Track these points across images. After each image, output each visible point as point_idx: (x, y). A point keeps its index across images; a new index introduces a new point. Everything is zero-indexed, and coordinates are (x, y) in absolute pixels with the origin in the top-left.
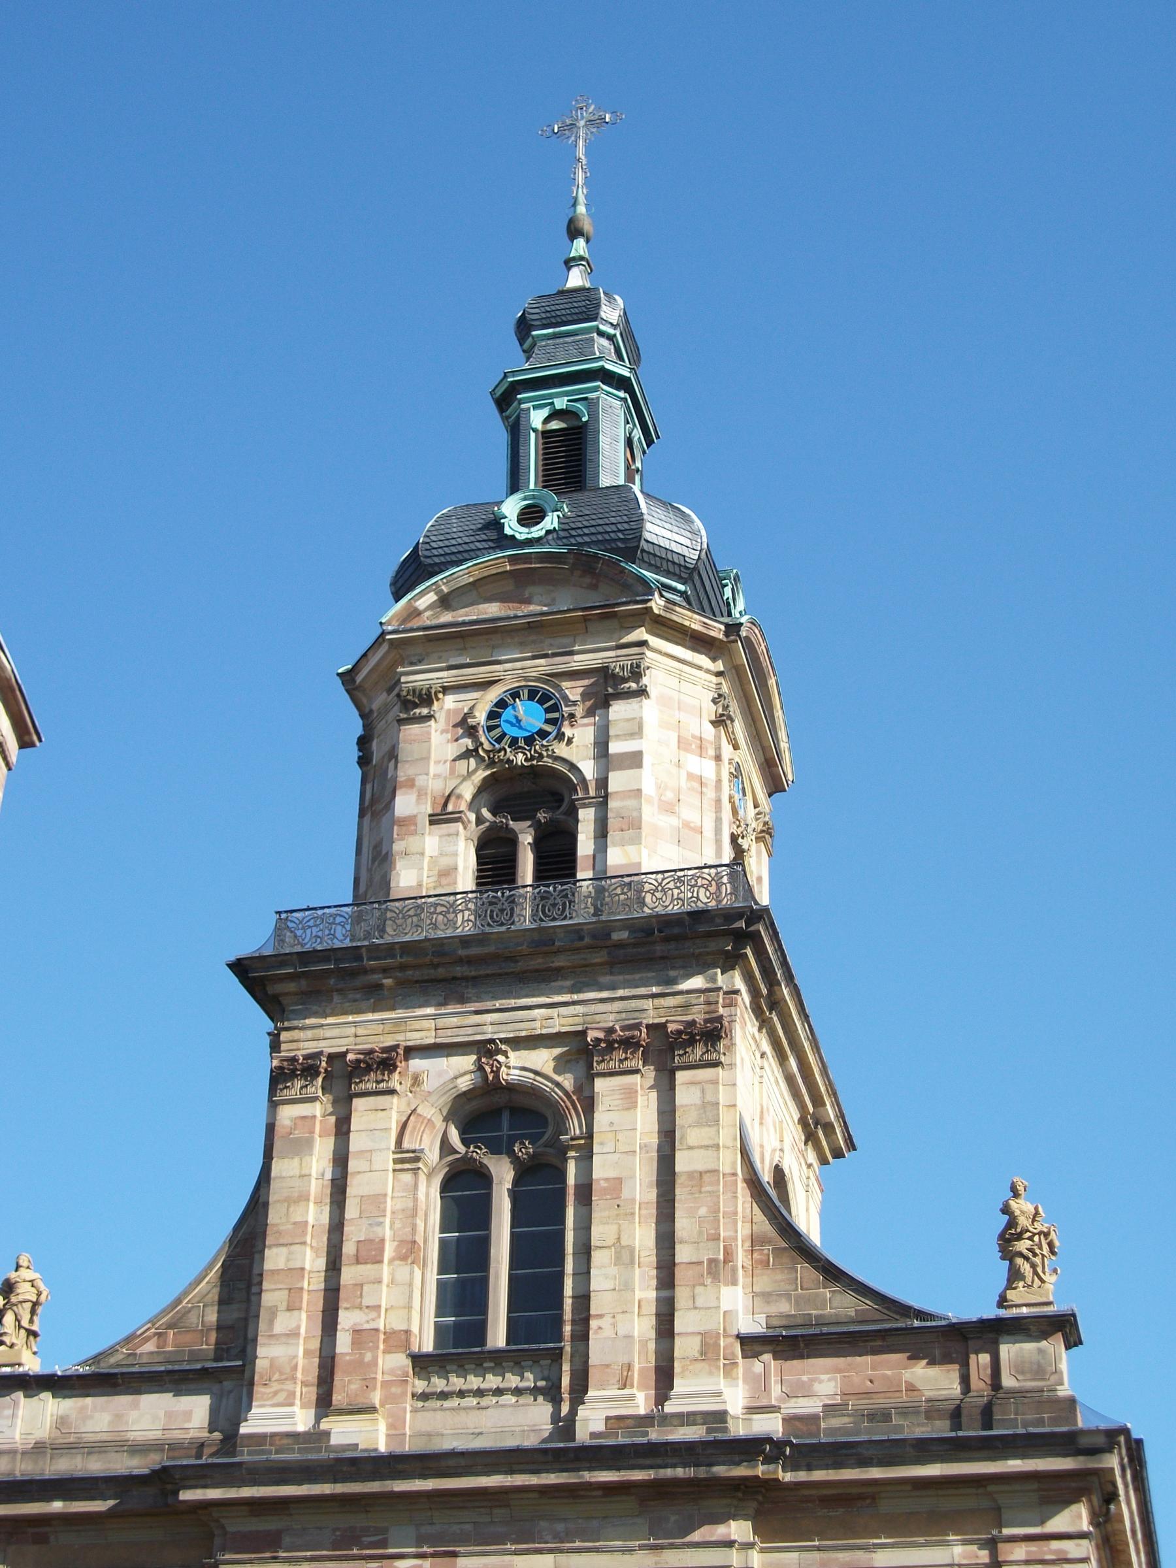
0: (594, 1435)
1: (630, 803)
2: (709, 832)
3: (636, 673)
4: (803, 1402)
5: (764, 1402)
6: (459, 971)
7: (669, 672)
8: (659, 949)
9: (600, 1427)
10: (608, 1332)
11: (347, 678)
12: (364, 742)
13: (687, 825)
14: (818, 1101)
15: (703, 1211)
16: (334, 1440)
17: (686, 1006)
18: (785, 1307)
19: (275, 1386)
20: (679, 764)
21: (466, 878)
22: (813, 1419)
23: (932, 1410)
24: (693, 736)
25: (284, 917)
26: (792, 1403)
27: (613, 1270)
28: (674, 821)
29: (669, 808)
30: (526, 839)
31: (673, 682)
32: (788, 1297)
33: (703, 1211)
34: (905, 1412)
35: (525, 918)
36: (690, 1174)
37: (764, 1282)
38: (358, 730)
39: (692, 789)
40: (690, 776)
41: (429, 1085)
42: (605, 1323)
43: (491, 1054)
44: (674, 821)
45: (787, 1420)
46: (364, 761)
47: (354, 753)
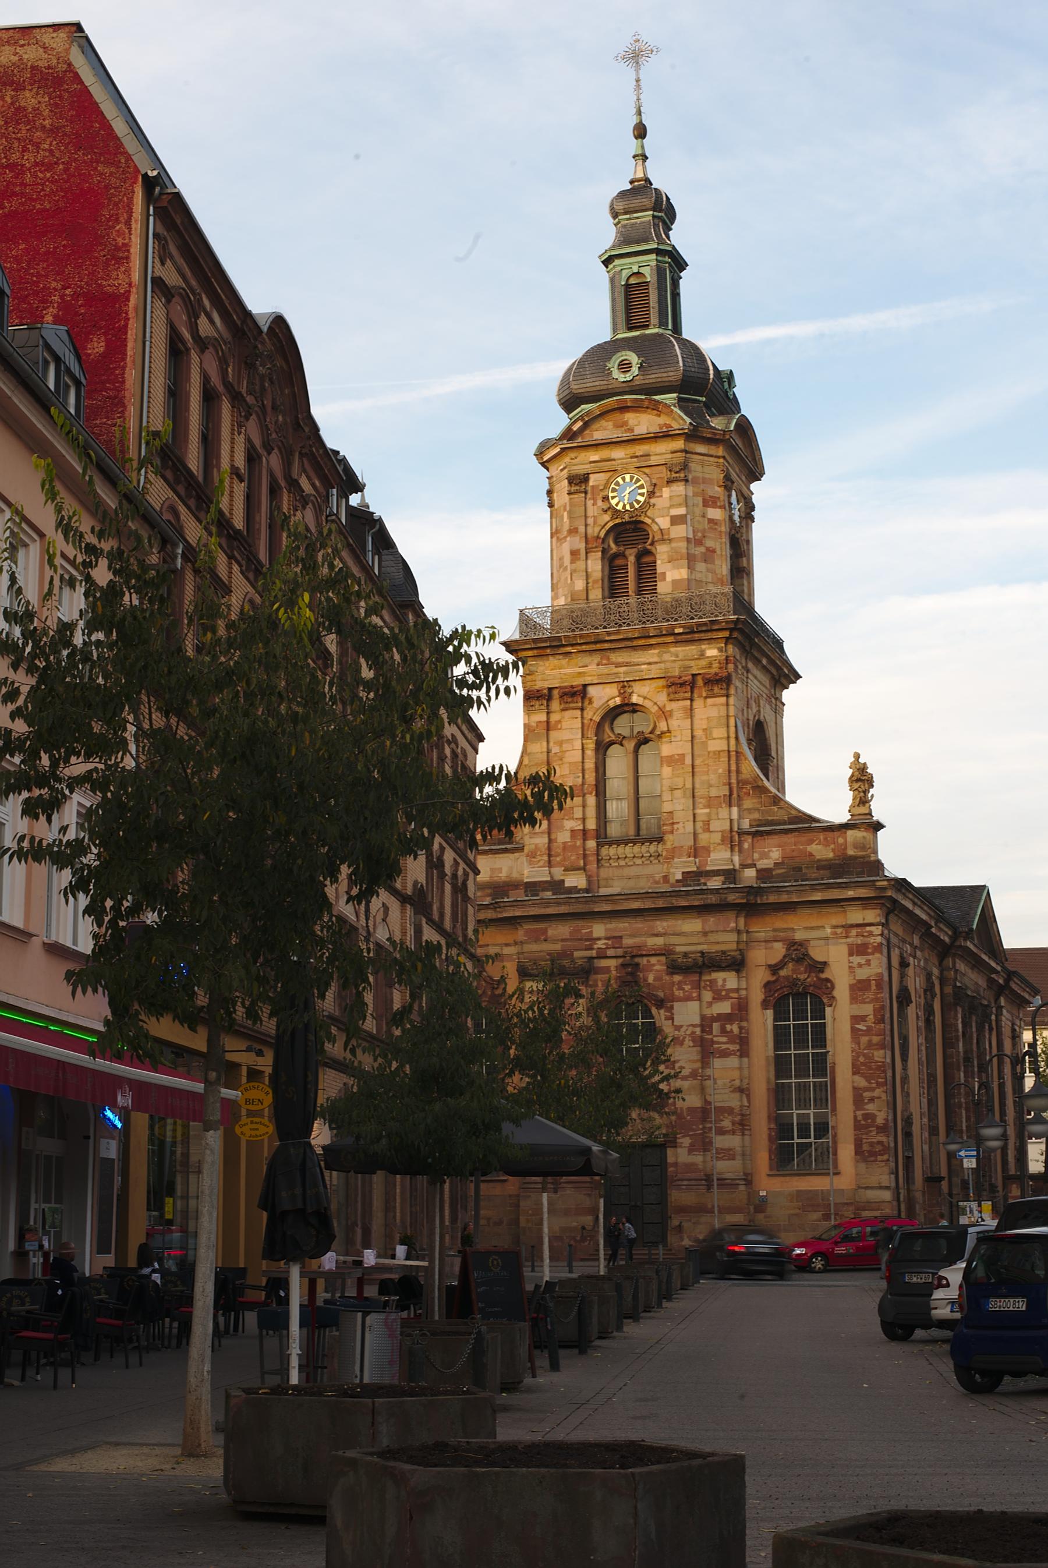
0: (678, 881)
4: (765, 861)
5: (749, 862)
6: (606, 646)
7: (697, 463)
9: (679, 877)
10: (681, 831)
12: (550, 493)
13: (708, 549)
14: (779, 669)
15: (720, 771)
16: (567, 885)
17: (710, 665)
18: (756, 816)
19: (539, 858)
20: (704, 516)
22: (768, 870)
23: (823, 865)
24: (711, 497)
26: (761, 862)
27: (683, 801)
28: (702, 549)
29: (699, 542)
30: (632, 559)
32: (758, 810)
33: (720, 771)
36: (714, 752)
38: (547, 487)
39: (711, 528)
40: (711, 521)
41: (597, 704)
43: (624, 687)
44: (702, 549)
45: (757, 871)
46: (551, 505)
47: (546, 500)
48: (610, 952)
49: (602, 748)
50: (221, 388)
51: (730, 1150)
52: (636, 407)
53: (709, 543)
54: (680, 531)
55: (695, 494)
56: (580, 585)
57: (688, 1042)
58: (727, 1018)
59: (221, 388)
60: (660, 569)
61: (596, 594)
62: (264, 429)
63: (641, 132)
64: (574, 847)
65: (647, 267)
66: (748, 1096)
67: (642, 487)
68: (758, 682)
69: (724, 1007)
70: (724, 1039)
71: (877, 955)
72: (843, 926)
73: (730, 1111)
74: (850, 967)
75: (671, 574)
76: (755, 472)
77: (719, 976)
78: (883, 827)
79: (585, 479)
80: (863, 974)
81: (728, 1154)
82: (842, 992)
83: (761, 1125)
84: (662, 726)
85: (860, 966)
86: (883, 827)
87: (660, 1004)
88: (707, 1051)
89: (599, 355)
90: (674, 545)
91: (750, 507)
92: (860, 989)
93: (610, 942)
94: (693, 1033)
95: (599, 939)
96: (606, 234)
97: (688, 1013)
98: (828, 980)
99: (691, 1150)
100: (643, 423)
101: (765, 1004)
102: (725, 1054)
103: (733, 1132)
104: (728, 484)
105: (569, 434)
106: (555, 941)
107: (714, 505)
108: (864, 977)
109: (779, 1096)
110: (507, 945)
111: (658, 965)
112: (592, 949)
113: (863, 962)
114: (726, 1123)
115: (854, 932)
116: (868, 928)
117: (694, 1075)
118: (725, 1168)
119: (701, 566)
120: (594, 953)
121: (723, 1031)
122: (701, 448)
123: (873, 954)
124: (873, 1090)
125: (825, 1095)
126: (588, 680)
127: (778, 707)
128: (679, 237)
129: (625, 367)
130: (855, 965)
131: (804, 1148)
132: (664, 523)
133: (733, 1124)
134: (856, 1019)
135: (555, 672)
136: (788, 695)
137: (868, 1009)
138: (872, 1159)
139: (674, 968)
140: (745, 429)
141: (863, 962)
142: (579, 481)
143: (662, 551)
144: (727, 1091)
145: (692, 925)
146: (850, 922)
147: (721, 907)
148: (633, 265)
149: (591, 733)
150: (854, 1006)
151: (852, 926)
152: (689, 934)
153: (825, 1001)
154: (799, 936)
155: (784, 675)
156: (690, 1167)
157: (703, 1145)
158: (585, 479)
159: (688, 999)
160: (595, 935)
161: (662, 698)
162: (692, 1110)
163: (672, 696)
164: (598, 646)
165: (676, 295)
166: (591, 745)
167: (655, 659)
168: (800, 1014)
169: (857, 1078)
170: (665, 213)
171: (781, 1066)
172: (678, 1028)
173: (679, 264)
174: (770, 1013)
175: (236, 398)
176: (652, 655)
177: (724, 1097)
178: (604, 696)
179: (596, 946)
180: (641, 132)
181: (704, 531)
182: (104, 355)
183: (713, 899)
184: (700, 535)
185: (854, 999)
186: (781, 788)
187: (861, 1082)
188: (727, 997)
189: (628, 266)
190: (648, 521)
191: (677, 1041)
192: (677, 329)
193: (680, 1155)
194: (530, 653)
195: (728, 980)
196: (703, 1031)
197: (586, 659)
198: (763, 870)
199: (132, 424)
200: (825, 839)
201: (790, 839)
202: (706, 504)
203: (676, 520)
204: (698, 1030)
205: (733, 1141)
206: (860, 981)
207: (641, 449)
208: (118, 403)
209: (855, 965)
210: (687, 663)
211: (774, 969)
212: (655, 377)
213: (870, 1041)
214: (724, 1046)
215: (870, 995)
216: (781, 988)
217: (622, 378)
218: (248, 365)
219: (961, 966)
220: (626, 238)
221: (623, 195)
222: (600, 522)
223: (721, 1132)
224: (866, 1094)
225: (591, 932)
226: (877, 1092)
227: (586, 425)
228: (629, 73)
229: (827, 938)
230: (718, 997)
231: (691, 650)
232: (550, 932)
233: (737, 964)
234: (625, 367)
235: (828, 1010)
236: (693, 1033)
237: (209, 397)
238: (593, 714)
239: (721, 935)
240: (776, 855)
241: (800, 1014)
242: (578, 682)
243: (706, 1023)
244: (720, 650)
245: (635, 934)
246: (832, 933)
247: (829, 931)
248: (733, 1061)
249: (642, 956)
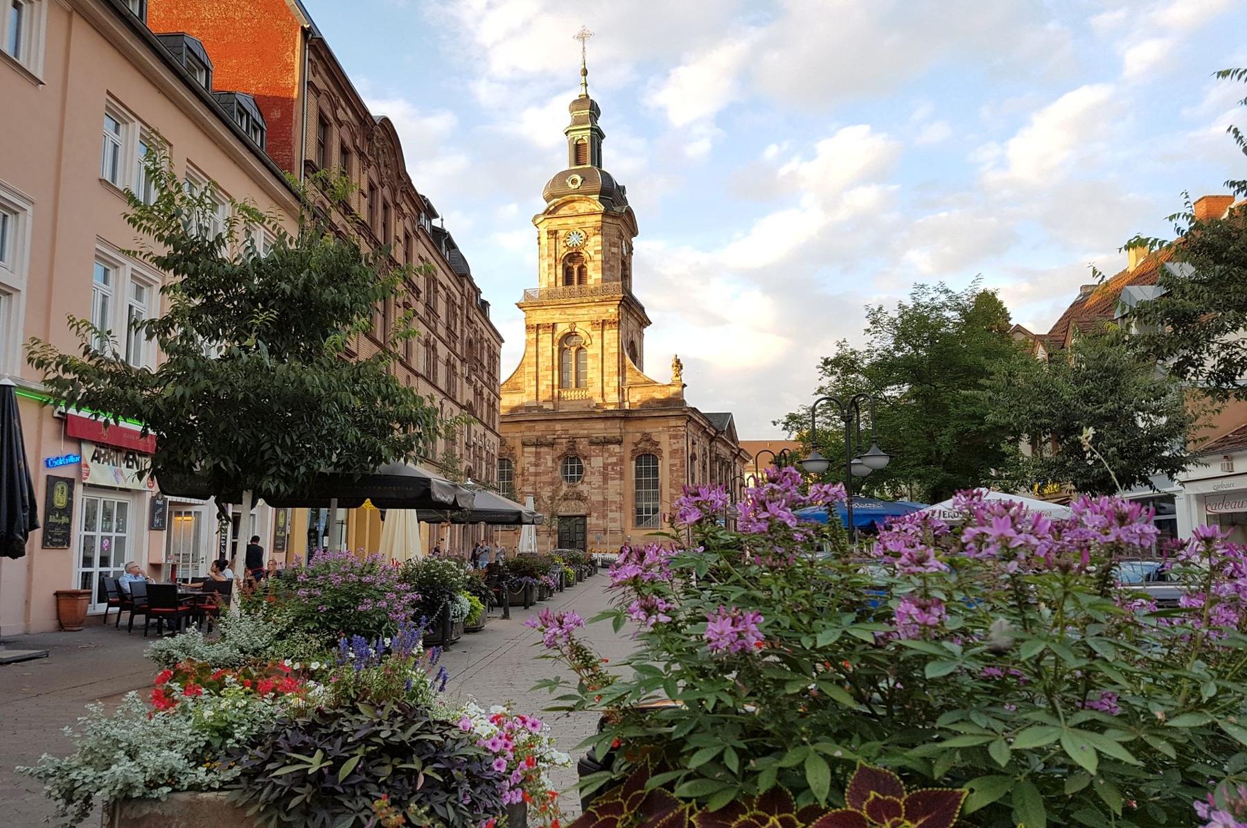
49: (562, 350)
50: (352, 149)
52: (580, 200)
54: (599, 257)
56: (553, 279)
58: (615, 464)
59: (352, 149)
61: (560, 283)
62: (380, 175)
63: (585, 73)
65: (585, 136)
68: (632, 324)
69: (614, 460)
75: (594, 275)
76: (634, 232)
77: (611, 447)
79: (556, 232)
81: (614, 520)
83: (630, 510)
84: (588, 342)
87: (585, 458)
88: (605, 478)
89: (563, 175)
91: (631, 249)
96: (567, 120)
97: (597, 462)
100: (582, 207)
101: (632, 459)
104: (621, 236)
105: (547, 212)
109: (638, 496)
111: (585, 442)
114: (614, 508)
117: (599, 487)
118: (612, 526)
119: (608, 273)
122: (610, 221)
125: (657, 497)
127: (641, 336)
128: (601, 123)
129: (574, 182)
131: (647, 518)
132: (592, 253)
136: (646, 331)
139: (592, 443)
140: (630, 213)
142: (553, 233)
145: (600, 425)
147: (614, 418)
148: (578, 135)
149: (556, 343)
152: (599, 429)
154: (647, 431)
155: (644, 322)
157: (604, 516)
158: (556, 232)
161: (589, 330)
165: (599, 150)
166: (556, 349)
168: (647, 463)
170: (595, 111)
171: (638, 484)
173: (602, 136)
174: (634, 463)
175: (361, 155)
176: (584, 311)
178: (562, 328)
180: (585, 73)
182: (280, 120)
183: (609, 415)
186: (642, 369)
189: (578, 135)
192: (599, 166)
195: (615, 448)
199: (297, 155)
201: (644, 390)
203: (596, 252)
205: (617, 515)
207: (581, 219)
208: (288, 144)
211: (636, 444)
212: (587, 188)
217: (572, 187)
218: (369, 138)
219: (719, 445)
220: (577, 121)
221: (575, 102)
222: (563, 252)
227: (557, 208)
228: (579, 44)
230: (611, 455)
231: (603, 309)
233: (619, 442)
234: (574, 182)
237: (344, 151)
238: (558, 336)
239: (613, 429)
240: (638, 397)
241: (647, 463)
242: (551, 322)
243: (605, 467)
245: (575, 429)
248: (617, 482)
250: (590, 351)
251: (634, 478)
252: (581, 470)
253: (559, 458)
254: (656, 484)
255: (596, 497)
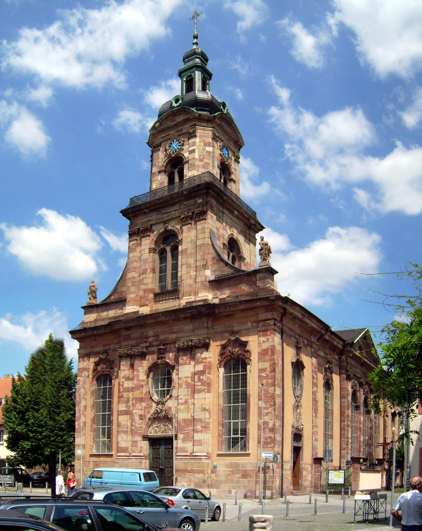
1: (193, 161)
2: (211, 164)
3: (194, 132)
8: (193, 195)
11: (148, 143)
13: (206, 163)
15: (201, 253)
18: (218, 273)
20: (204, 150)
21: (166, 184)
25: (131, 200)
27: (186, 269)
28: (203, 163)
29: (201, 160)
31: (203, 131)
34: (241, 295)
35: (176, 190)
37: (215, 267)
40: (207, 152)
42: (184, 281)
44: (203, 163)
47: (150, 159)
48: (154, 343)
51: (200, 441)
53: (206, 160)
55: (200, 142)
57: (184, 386)
58: (202, 372)
60: (185, 174)
64: (145, 297)
66: (209, 413)
67: (180, 142)
69: (200, 367)
70: (199, 384)
71: (272, 336)
72: (256, 322)
73: (200, 420)
74: (259, 343)
75: (188, 173)
78: (277, 272)
80: (265, 346)
81: (200, 443)
82: (254, 357)
85: (264, 342)
86: (277, 272)
90: (190, 162)
92: (263, 355)
93: (154, 338)
94: (186, 381)
95: (150, 337)
98: (248, 351)
99: (184, 440)
102: (200, 391)
103: (202, 431)
106: (132, 339)
107: (209, 146)
108: (265, 348)
110: (117, 344)
112: (146, 342)
113: (265, 340)
114: (199, 427)
115: (261, 324)
116: (268, 322)
117: (186, 402)
118: (199, 451)
120: (148, 344)
121: (199, 380)
123: (270, 335)
124: (267, 408)
126: (152, 222)
130: (261, 341)
133: (202, 427)
134: (261, 370)
135: (141, 222)
137: (267, 365)
138: (266, 446)
141: (265, 340)
143: (186, 167)
144: (200, 410)
146: (259, 319)
150: (260, 364)
151: (260, 321)
153: (247, 361)
156: (184, 450)
159: (185, 364)
160: (149, 335)
162: (185, 420)
163: (183, 224)
164: (156, 207)
167: (178, 208)
169: (260, 402)
172: (179, 379)
174: (222, 370)
177: (199, 415)
179: (149, 341)
181: (204, 156)
184: (202, 157)
185: (260, 360)
187: (262, 404)
188: (202, 362)
190: (181, 156)
191: (180, 386)
193: (178, 444)
194: (131, 215)
196: (191, 380)
197: (152, 214)
198: (222, 299)
200: (247, 280)
202: (205, 145)
204: (189, 380)
206: (264, 350)
209: (261, 341)
210: (189, 208)
213: (267, 382)
214: (199, 387)
215: (268, 357)
216: (227, 356)
223: (197, 432)
224: (265, 411)
225: (147, 334)
226: (270, 410)
229: (248, 329)
230: (198, 363)
232: (132, 336)
235: (248, 367)
236: (186, 381)
244: (203, 199)
246: (251, 326)
247: (250, 325)
249: (168, 344)
250: (180, 248)
251: (221, 390)
252: (170, 381)
253: (150, 369)
254: (245, 398)
255: (182, 416)
